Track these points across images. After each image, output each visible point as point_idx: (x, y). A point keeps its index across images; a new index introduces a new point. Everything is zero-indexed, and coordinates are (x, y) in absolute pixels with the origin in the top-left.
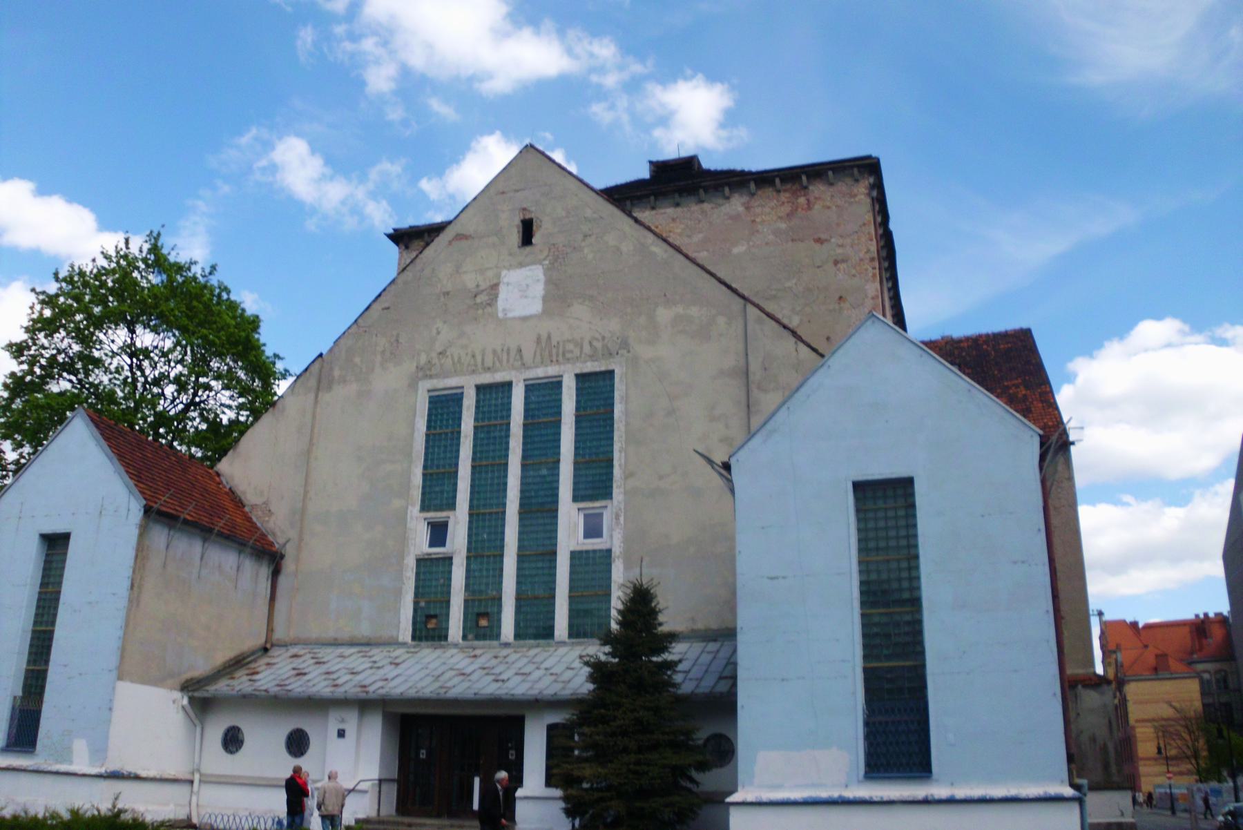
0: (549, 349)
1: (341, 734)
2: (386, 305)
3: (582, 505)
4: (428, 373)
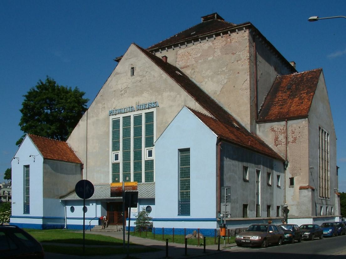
2: (101, 95)
3: (147, 148)
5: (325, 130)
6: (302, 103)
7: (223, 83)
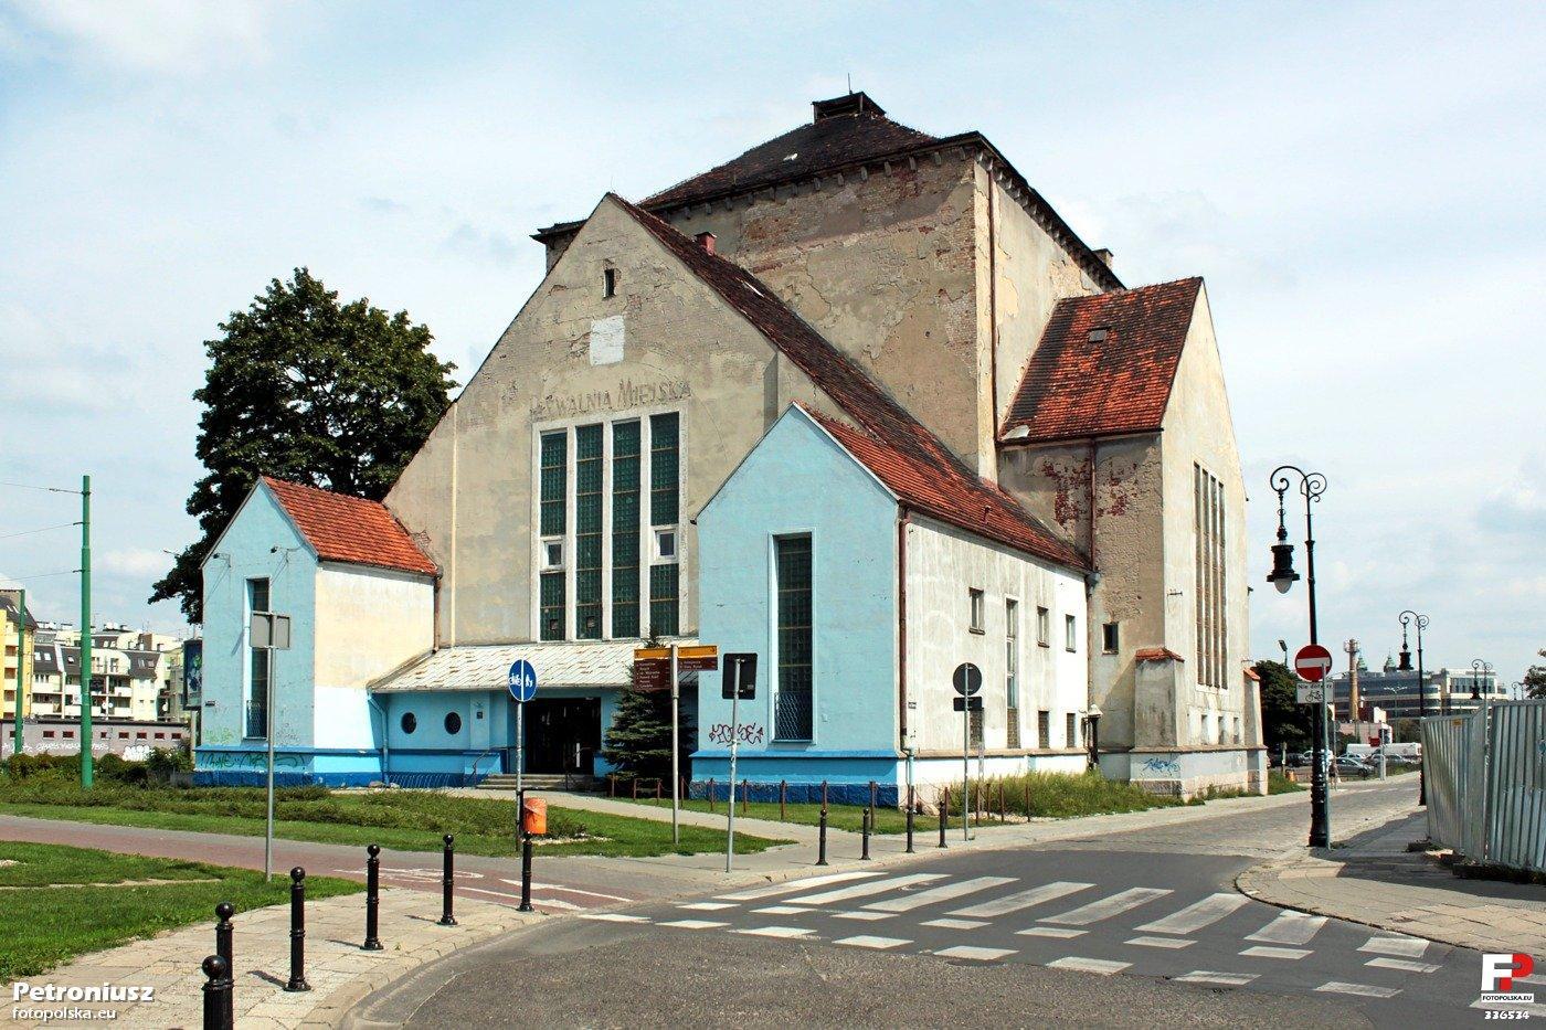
0: (630, 393)
1: (480, 716)
4: (539, 416)
5: (1210, 473)
6: (1142, 389)
7: (892, 323)
